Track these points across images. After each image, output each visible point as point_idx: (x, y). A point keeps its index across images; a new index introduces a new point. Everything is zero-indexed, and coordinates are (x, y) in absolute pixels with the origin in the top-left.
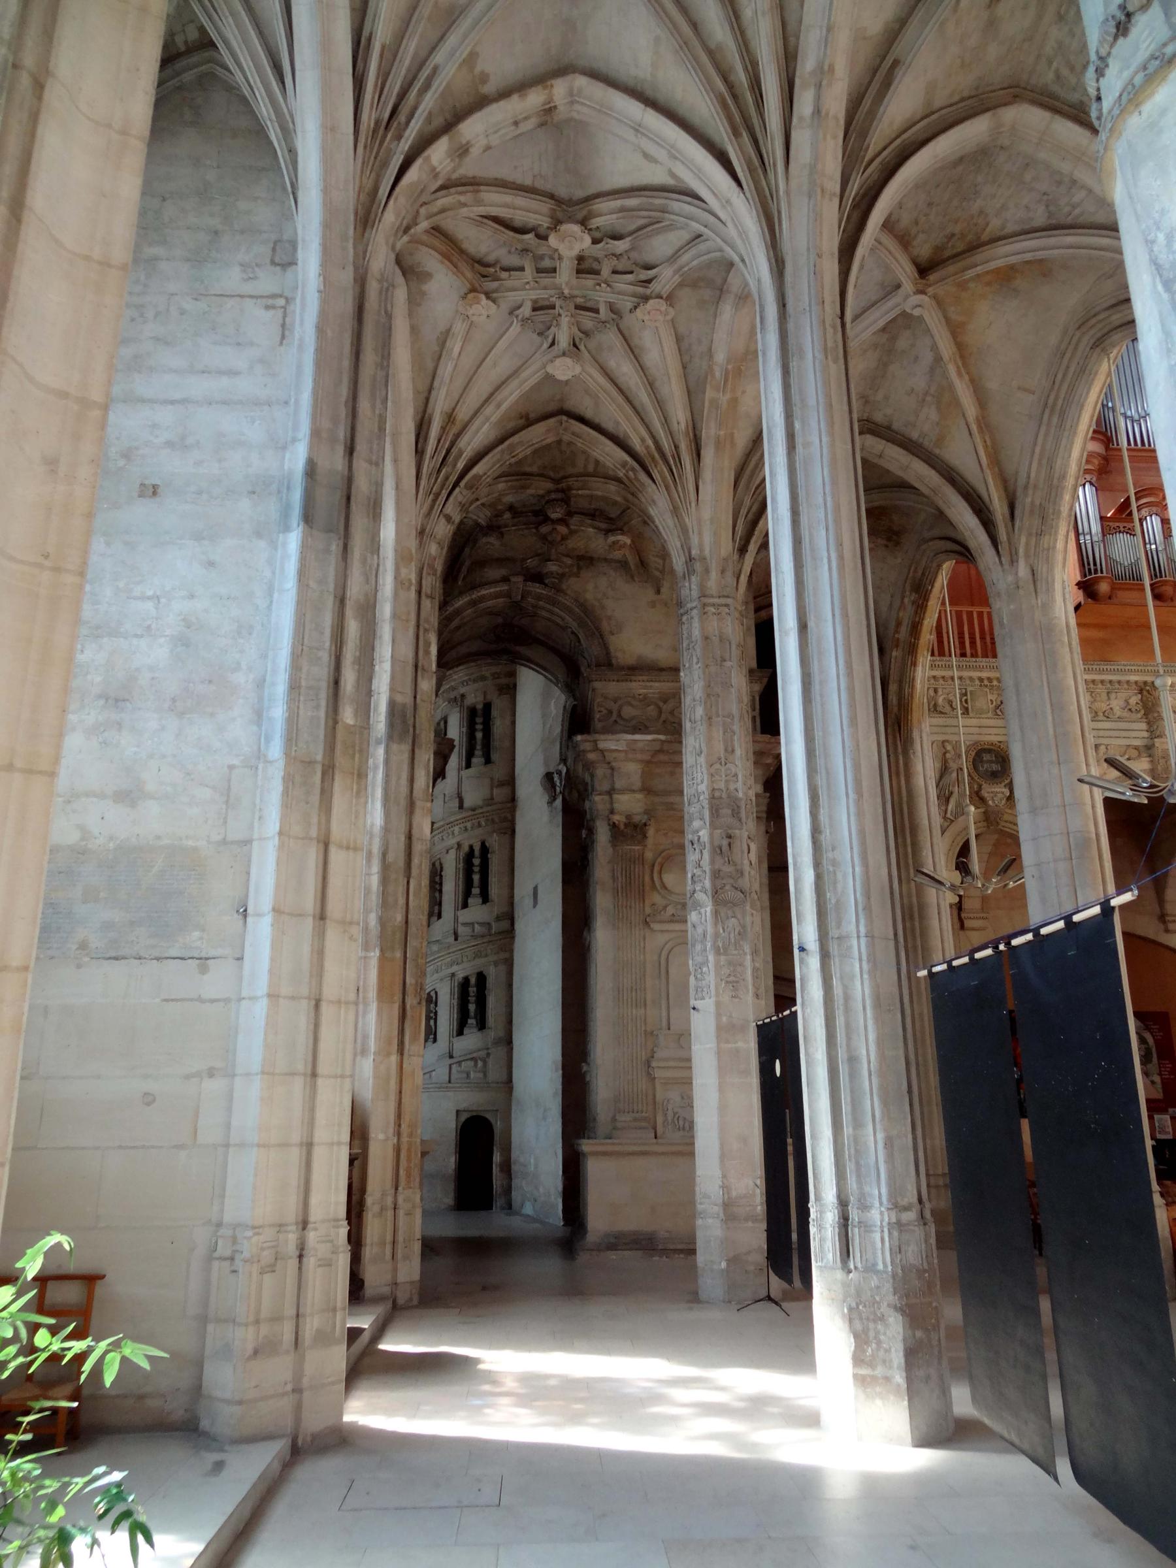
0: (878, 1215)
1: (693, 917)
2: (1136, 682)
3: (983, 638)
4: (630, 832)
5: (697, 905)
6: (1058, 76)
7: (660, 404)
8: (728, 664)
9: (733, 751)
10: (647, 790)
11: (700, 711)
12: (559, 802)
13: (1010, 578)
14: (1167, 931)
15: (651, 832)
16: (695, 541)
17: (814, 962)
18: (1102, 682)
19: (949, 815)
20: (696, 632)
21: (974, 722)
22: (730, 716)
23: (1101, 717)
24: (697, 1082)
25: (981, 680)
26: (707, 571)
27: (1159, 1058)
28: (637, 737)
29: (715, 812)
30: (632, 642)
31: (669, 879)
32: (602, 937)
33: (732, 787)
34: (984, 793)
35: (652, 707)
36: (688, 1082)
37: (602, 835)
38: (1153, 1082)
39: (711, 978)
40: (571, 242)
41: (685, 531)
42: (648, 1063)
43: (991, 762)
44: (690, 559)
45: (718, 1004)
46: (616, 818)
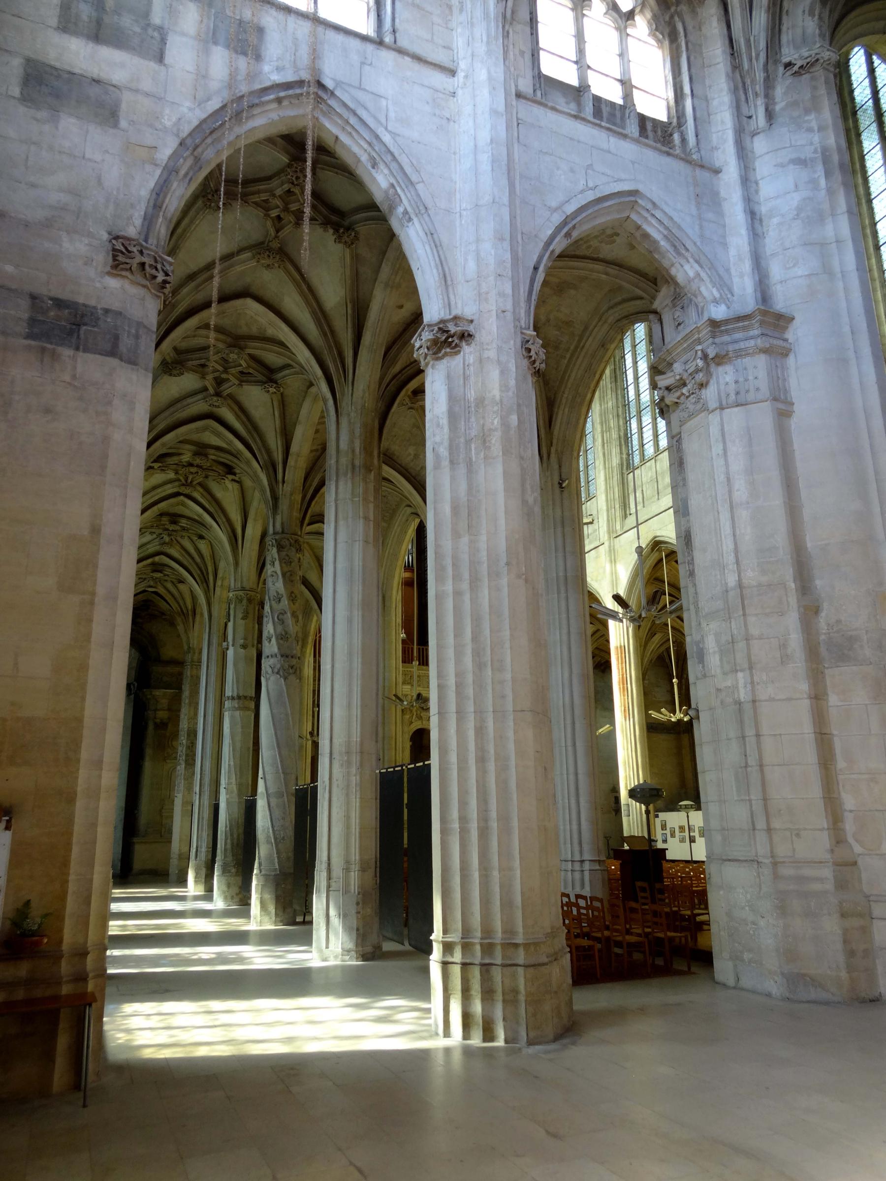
0: (204, 849)
1: (178, 768)
4: (162, 726)
5: (180, 764)
7: (183, 599)
10: (169, 710)
11: (187, 701)
12: (132, 696)
15: (170, 725)
16: (191, 641)
17: (198, 796)
20: (189, 673)
24: (175, 819)
26: (194, 653)
29: (188, 735)
30: (168, 652)
31: (174, 743)
32: (148, 766)
36: (172, 817)
37: (151, 727)
39: (182, 788)
40: (158, 575)
41: (188, 638)
42: (161, 811)
44: (189, 647)
45: (183, 796)
46: (158, 721)
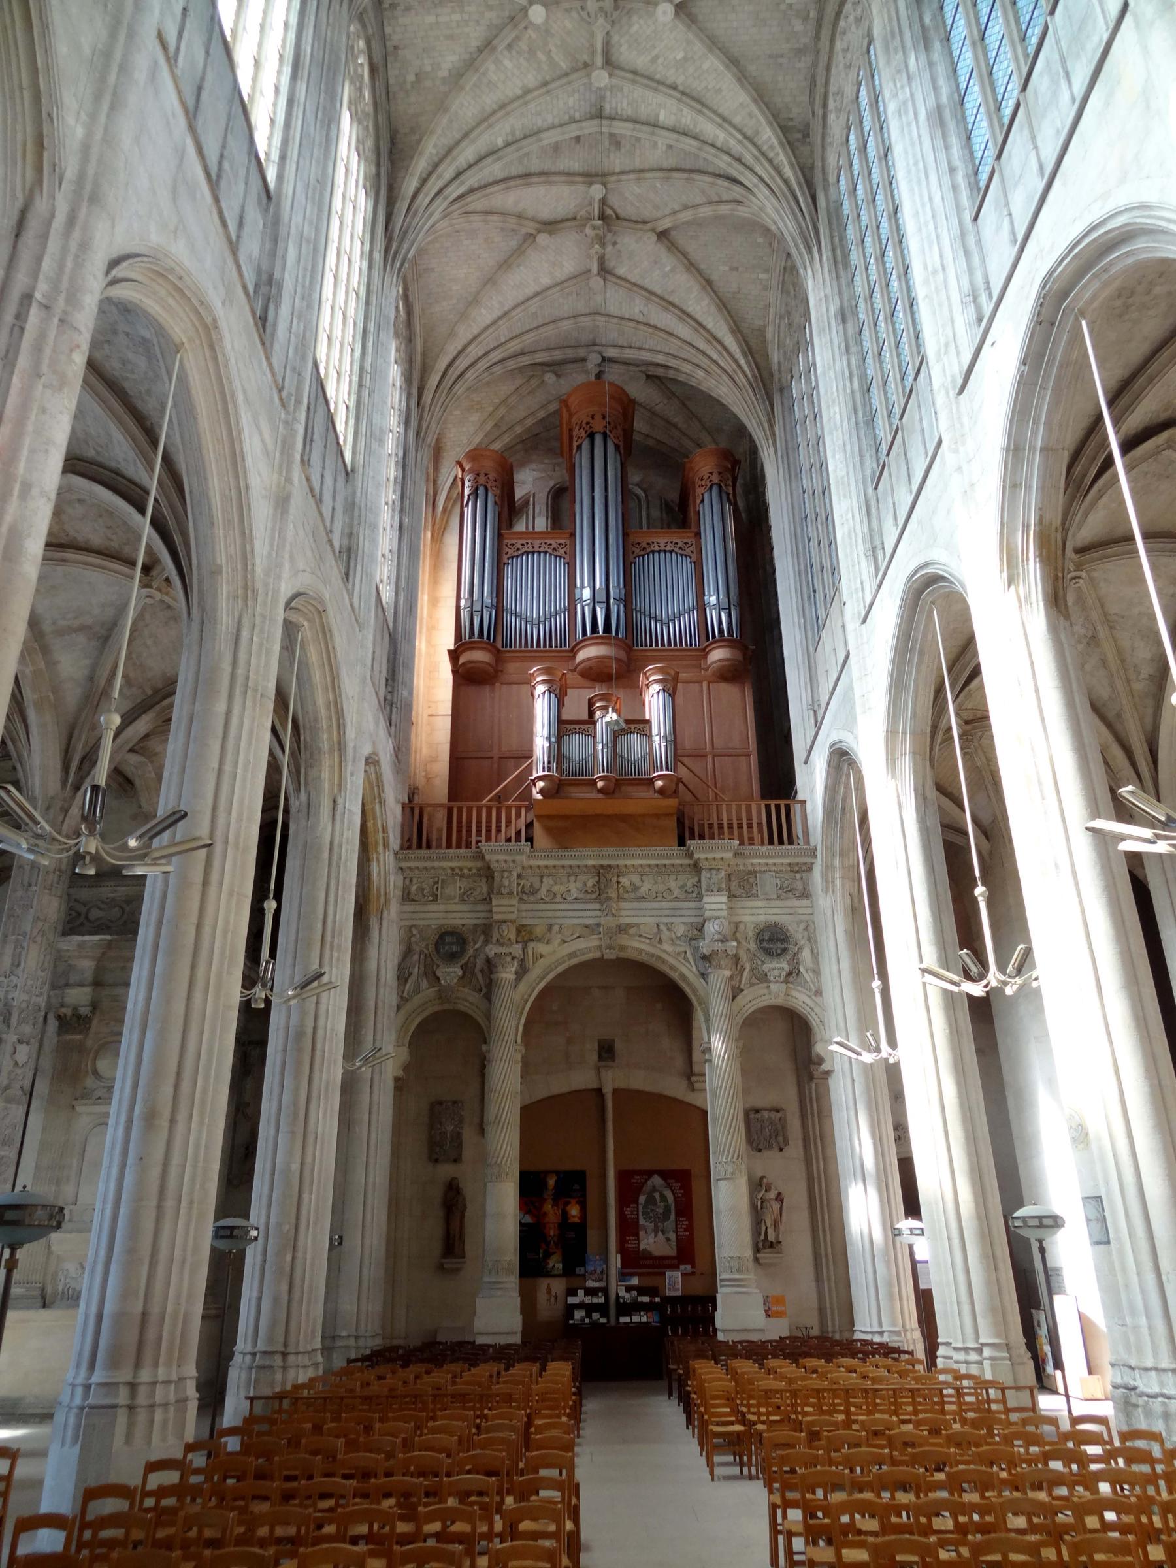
2: (594, 866)
3: (459, 831)
6: (98, 453)
8: (34, 888)
9: (18, 965)
13: (297, 803)
14: (693, 1090)
15: (95, 1022)
18: (563, 867)
19: (405, 995)
21: (442, 907)
22: (24, 934)
23: (559, 898)
25: (453, 869)
27: (677, 1215)
28: (87, 938)
31: (102, 1065)
33: (10, 997)
34: (439, 974)
35: (117, 909)
38: (668, 1240)
43: (452, 944)
